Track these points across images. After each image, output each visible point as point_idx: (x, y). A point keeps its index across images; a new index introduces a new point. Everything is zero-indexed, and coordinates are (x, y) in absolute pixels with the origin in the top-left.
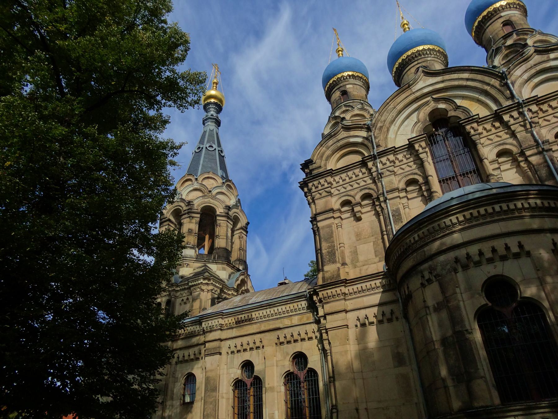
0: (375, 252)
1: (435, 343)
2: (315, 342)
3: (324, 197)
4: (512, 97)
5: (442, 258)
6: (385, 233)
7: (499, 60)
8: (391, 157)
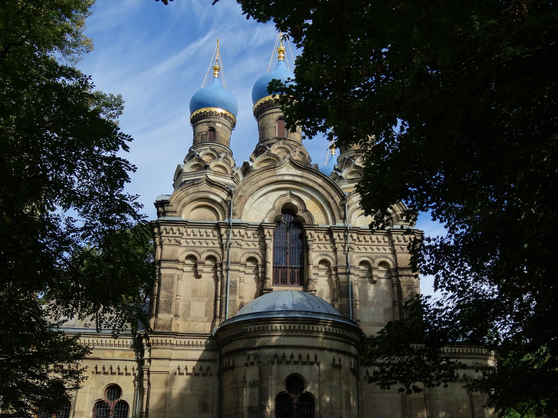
0: (206, 312)
1: (244, 408)
2: (133, 378)
3: (171, 245)
4: (344, 219)
5: (267, 352)
6: (219, 298)
7: (346, 174)
8: (243, 232)
